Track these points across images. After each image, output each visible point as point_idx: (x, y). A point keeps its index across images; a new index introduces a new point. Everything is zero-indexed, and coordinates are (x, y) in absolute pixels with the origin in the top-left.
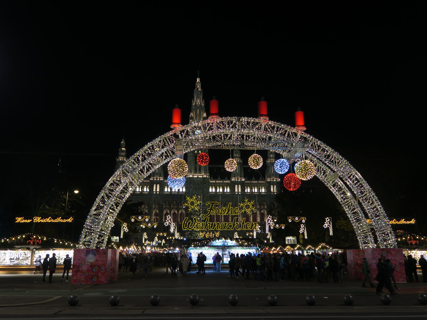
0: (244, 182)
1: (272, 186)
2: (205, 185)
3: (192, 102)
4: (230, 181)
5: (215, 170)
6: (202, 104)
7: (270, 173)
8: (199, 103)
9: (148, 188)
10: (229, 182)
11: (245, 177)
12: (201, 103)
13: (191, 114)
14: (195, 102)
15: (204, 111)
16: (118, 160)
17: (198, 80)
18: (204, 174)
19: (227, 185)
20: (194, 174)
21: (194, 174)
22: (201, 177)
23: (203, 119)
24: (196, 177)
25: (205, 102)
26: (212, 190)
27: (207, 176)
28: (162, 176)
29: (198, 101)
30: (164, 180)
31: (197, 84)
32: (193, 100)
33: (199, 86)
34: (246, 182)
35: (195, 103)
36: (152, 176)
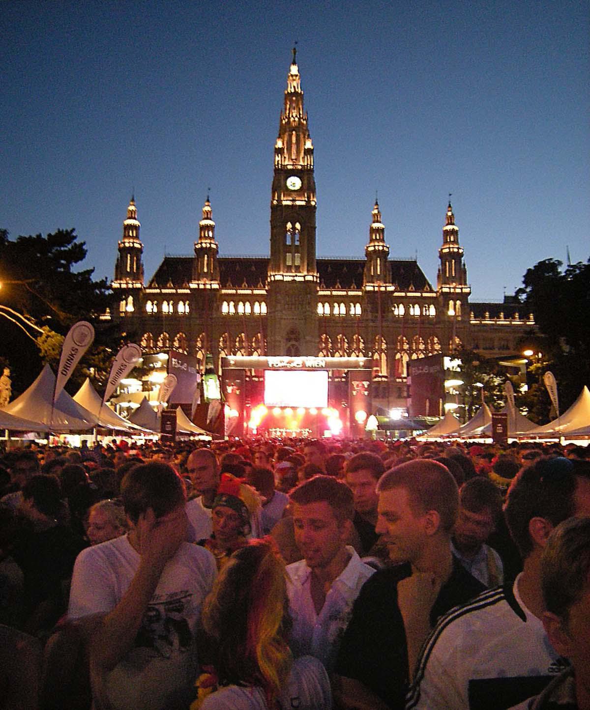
0: (393, 292)
1: (451, 303)
2: (309, 296)
6: (304, 120)
7: (448, 276)
8: (297, 119)
9: (186, 305)
10: (360, 293)
12: (299, 119)
14: (286, 118)
18: (305, 273)
19: (355, 300)
20: (285, 274)
21: (285, 274)
22: (302, 279)
23: (305, 153)
24: (290, 279)
26: (323, 309)
27: (313, 276)
28: (215, 280)
29: (294, 116)
30: (220, 289)
34: (396, 294)
36: (195, 280)
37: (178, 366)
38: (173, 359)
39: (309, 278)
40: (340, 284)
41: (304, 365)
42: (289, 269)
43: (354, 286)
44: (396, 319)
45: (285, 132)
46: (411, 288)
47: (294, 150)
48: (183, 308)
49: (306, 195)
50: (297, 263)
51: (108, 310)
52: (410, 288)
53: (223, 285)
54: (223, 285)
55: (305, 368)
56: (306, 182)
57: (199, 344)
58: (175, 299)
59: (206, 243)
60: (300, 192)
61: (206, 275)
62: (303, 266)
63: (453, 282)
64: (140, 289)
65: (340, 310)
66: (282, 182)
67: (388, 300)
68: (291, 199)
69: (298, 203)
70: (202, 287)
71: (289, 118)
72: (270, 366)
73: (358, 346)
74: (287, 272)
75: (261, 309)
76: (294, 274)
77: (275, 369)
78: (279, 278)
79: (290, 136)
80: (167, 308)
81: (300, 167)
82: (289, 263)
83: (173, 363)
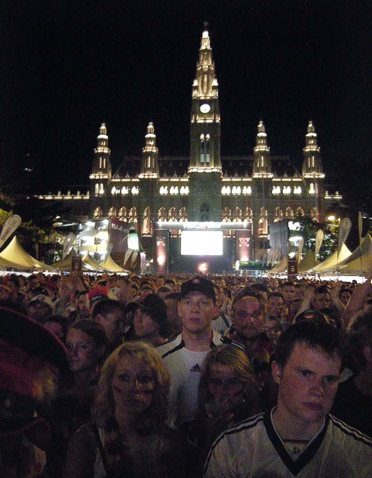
0: (271, 179)
1: (312, 185)
3: (196, 65)
4: (252, 178)
5: (231, 164)
6: (212, 67)
10: (250, 180)
11: (272, 172)
12: (209, 66)
13: (196, 83)
15: (214, 78)
16: (96, 152)
17: (205, 34)
19: (247, 184)
22: (210, 171)
25: (215, 65)
26: (225, 191)
31: (203, 40)
32: (198, 63)
33: (206, 44)
35: (201, 67)
37: (116, 228)
38: (112, 224)
39: (215, 170)
40: (238, 174)
41: (207, 228)
42: (202, 164)
43: (247, 174)
44: (275, 197)
45: (200, 75)
46: (286, 175)
47: (205, 88)
48: (135, 191)
49: (213, 117)
50: (208, 160)
51: (88, 193)
52: (285, 175)
53: (161, 175)
54: (161, 175)
55: (207, 229)
56: (213, 107)
57: (145, 214)
58: (130, 185)
59: (149, 149)
60: (210, 114)
61: (149, 169)
62: (211, 163)
63: (313, 171)
64: (107, 180)
65: (236, 191)
66: (198, 108)
67: (269, 184)
68: (203, 119)
69: (208, 121)
70: (146, 177)
71: (202, 66)
72: (185, 228)
73: (249, 214)
74: (201, 166)
75: (185, 191)
76: (205, 168)
77: (186, 229)
78: (195, 170)
79: (203, 77)
80: (125, 191)
81: (208, 98)
82: (202, 161)
83: (113, 226)
